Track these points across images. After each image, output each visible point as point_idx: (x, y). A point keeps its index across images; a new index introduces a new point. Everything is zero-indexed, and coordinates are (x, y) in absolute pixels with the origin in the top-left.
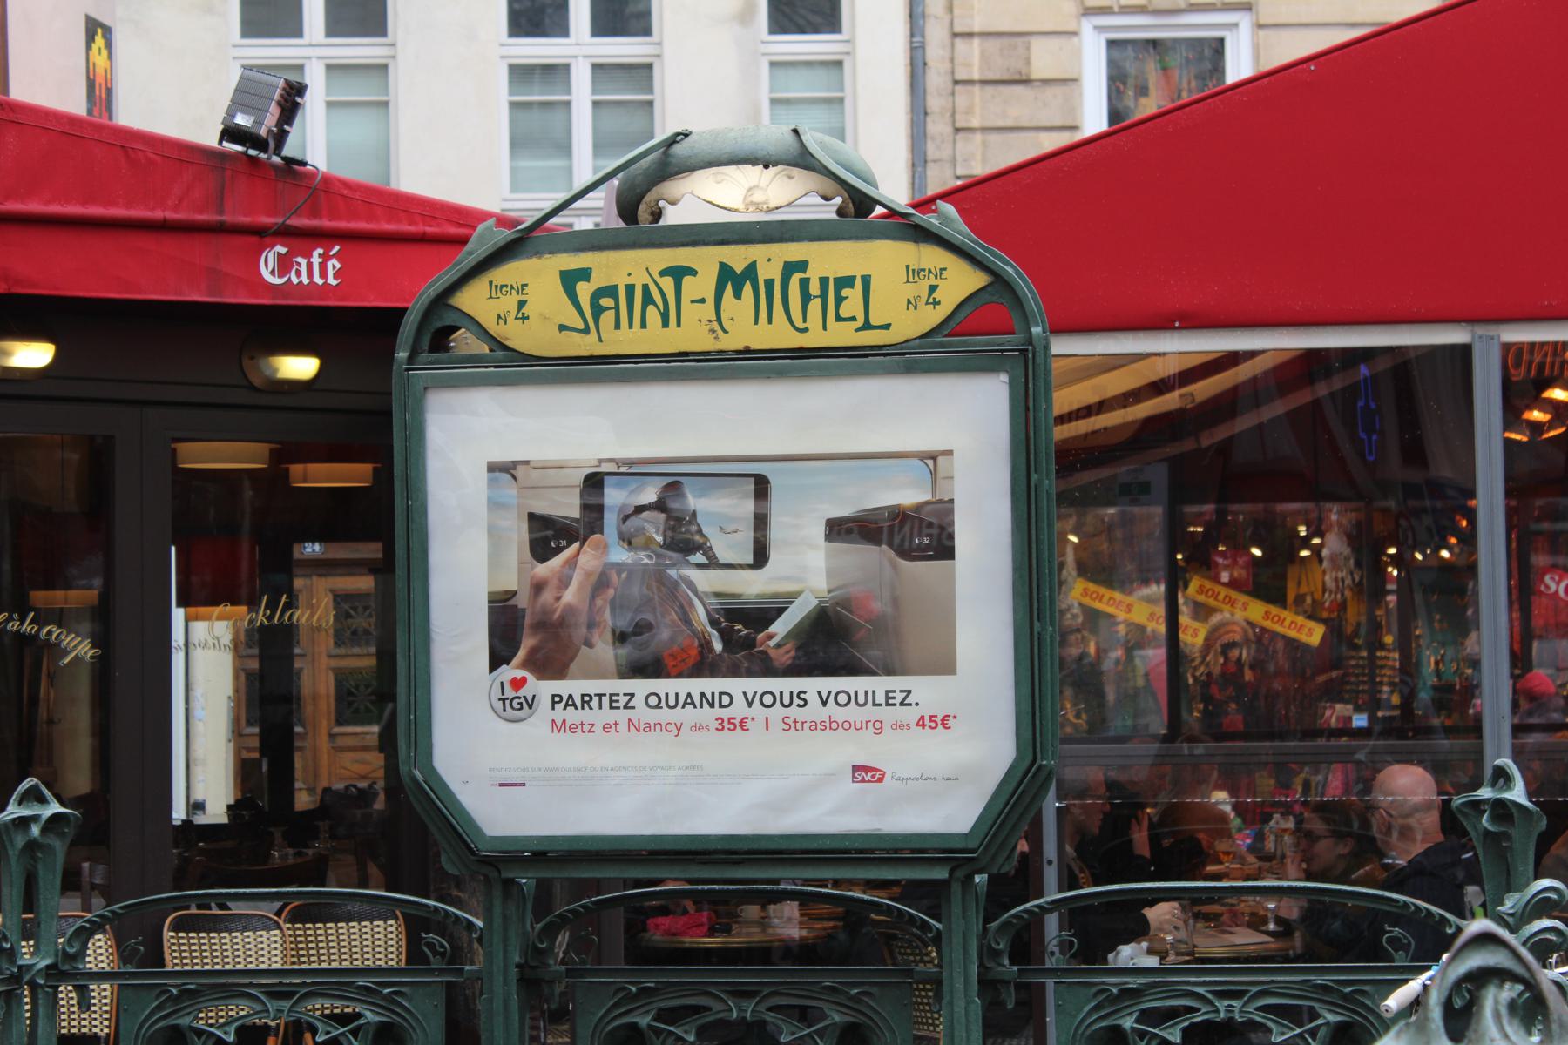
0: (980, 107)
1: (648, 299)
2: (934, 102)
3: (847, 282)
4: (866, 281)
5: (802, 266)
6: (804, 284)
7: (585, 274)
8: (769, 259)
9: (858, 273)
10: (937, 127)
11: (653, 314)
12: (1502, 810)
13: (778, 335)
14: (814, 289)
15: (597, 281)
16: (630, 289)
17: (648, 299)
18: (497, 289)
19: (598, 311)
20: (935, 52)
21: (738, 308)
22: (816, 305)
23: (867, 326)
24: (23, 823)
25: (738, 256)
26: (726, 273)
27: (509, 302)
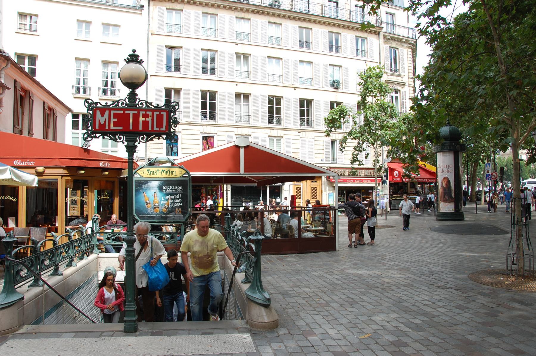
9: (174, 171)
12: (228, 218)
15: (151, 171)
18: (141, 171)
21: (164, 173)
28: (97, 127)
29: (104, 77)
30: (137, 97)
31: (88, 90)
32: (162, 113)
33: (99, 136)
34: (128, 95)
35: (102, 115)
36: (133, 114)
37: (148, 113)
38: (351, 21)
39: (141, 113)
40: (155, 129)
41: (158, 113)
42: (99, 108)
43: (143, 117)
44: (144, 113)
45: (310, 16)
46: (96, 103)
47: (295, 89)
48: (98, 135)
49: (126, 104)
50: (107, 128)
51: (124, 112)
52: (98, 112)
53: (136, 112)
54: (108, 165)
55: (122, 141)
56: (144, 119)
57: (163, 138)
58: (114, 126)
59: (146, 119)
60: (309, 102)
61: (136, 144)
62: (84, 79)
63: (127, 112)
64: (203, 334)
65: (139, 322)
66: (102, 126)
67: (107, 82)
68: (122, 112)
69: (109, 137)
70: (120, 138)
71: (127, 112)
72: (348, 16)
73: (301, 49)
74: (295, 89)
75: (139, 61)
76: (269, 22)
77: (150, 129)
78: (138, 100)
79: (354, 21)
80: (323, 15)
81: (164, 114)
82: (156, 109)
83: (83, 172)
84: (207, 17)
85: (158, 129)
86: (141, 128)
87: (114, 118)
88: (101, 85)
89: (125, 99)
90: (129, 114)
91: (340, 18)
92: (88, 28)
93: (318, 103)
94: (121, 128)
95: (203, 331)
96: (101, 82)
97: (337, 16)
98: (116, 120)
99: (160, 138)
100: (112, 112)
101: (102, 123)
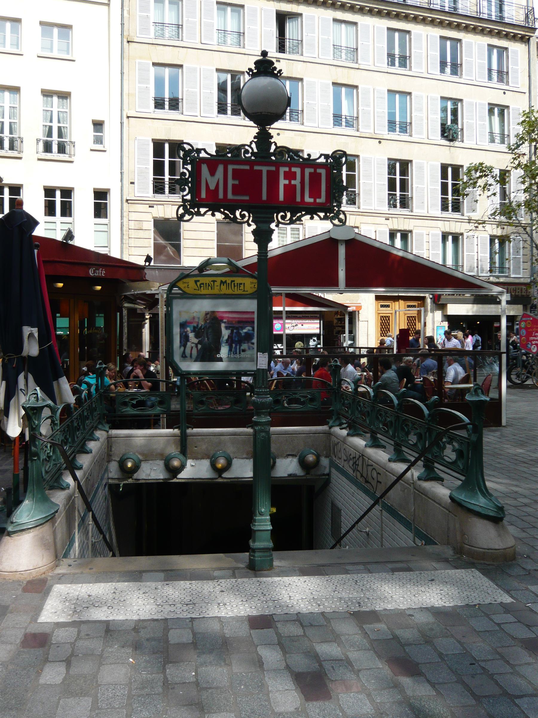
0: (133, 234)
1: (209, 285)
2: (124, 233)
3: (241, 284)
4: (244, 284)
5: (234, 281)
6: (234, 284)
7: (199, 281)
8: (229, 280)
10: (125, 237)
11: (210, 288)
13: (230, 292)
14: (236, 285)
15: (201, 282)
16: (206, 284)
17: (209, 285)
19: (201, 287)
20: (125, 223)
21: (224, 287)
22: (236, 287)
23: (244, 291)
24: (100, 368)
25: (224, 279)
26: (222, 282)
27: (186, 285)
28: (203, 195)
29: (45, 119)
30: (272, 140)
31: (17, 144)
32: (319, 171)
33: (205, 213)
34: (255, 137)
35: (212, 173)
36: (268, 172)
37: (293, 169)
38: (481, 16)
39: (283, 170)
40: (308, 199)
41: (312, 170)
42: (204, 160)
43: (285, 178)
44: (287, 169)
45: (407, 8)
46: (199, 151)
47: (380, 142)
48: (203, 210)
49: (253, 153)
50: (221, 196)
51: (252, 168)
52: (205, 169)
53: (273, 168)
54: (101, 273)
55: (247, 222)
56: (287, 182)
57: (319, 216)
58: (234, 193)
59: (290, 182)
60: (405, 165)
61: (273, 226)
62: (10, 123)
63: (256, 168)
64: (393, 570)
65: (273, 551)
66: (213, 193)
67: (51, 128)
68: (247, 167)
69: (223, 213)
70: (243, 216)
71: (256, 168)
72: (475, 8)
73: (392, 70)
74: (380, 142)
75: (276, 72)
76: (335, 20)
77: (298, 199)
78: (273, 147)
79: (486, 16)
80: (431, 7)
81: (323, 172)
82: (306, 162)
83: (60, 285)
84: (225, 10)
85: (312, 200)
86: (281, 198)
87: (234, 178)
88: (41, 135)
89: (251, 143)
90: (261, 171)
91: (460, 11)
92: (15, 31)
93: (421, 168)
94: (247, 198)
95: (390, 566)
96: (41, 128)
97: (455, 9)
98: (237, 182)
99: (314, 216)
100: (230, 168)
101: (212, 187)
